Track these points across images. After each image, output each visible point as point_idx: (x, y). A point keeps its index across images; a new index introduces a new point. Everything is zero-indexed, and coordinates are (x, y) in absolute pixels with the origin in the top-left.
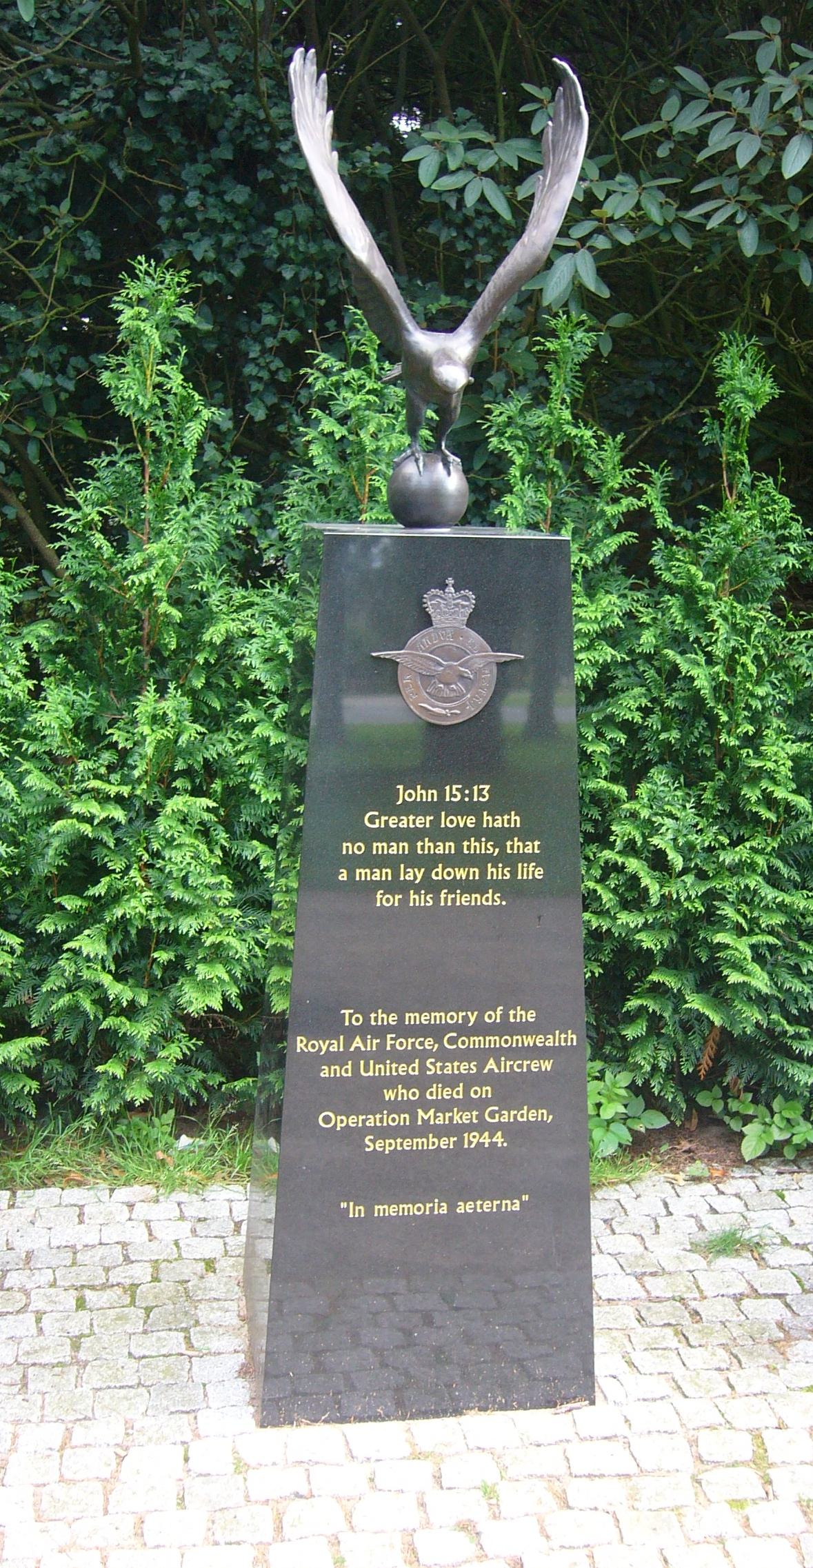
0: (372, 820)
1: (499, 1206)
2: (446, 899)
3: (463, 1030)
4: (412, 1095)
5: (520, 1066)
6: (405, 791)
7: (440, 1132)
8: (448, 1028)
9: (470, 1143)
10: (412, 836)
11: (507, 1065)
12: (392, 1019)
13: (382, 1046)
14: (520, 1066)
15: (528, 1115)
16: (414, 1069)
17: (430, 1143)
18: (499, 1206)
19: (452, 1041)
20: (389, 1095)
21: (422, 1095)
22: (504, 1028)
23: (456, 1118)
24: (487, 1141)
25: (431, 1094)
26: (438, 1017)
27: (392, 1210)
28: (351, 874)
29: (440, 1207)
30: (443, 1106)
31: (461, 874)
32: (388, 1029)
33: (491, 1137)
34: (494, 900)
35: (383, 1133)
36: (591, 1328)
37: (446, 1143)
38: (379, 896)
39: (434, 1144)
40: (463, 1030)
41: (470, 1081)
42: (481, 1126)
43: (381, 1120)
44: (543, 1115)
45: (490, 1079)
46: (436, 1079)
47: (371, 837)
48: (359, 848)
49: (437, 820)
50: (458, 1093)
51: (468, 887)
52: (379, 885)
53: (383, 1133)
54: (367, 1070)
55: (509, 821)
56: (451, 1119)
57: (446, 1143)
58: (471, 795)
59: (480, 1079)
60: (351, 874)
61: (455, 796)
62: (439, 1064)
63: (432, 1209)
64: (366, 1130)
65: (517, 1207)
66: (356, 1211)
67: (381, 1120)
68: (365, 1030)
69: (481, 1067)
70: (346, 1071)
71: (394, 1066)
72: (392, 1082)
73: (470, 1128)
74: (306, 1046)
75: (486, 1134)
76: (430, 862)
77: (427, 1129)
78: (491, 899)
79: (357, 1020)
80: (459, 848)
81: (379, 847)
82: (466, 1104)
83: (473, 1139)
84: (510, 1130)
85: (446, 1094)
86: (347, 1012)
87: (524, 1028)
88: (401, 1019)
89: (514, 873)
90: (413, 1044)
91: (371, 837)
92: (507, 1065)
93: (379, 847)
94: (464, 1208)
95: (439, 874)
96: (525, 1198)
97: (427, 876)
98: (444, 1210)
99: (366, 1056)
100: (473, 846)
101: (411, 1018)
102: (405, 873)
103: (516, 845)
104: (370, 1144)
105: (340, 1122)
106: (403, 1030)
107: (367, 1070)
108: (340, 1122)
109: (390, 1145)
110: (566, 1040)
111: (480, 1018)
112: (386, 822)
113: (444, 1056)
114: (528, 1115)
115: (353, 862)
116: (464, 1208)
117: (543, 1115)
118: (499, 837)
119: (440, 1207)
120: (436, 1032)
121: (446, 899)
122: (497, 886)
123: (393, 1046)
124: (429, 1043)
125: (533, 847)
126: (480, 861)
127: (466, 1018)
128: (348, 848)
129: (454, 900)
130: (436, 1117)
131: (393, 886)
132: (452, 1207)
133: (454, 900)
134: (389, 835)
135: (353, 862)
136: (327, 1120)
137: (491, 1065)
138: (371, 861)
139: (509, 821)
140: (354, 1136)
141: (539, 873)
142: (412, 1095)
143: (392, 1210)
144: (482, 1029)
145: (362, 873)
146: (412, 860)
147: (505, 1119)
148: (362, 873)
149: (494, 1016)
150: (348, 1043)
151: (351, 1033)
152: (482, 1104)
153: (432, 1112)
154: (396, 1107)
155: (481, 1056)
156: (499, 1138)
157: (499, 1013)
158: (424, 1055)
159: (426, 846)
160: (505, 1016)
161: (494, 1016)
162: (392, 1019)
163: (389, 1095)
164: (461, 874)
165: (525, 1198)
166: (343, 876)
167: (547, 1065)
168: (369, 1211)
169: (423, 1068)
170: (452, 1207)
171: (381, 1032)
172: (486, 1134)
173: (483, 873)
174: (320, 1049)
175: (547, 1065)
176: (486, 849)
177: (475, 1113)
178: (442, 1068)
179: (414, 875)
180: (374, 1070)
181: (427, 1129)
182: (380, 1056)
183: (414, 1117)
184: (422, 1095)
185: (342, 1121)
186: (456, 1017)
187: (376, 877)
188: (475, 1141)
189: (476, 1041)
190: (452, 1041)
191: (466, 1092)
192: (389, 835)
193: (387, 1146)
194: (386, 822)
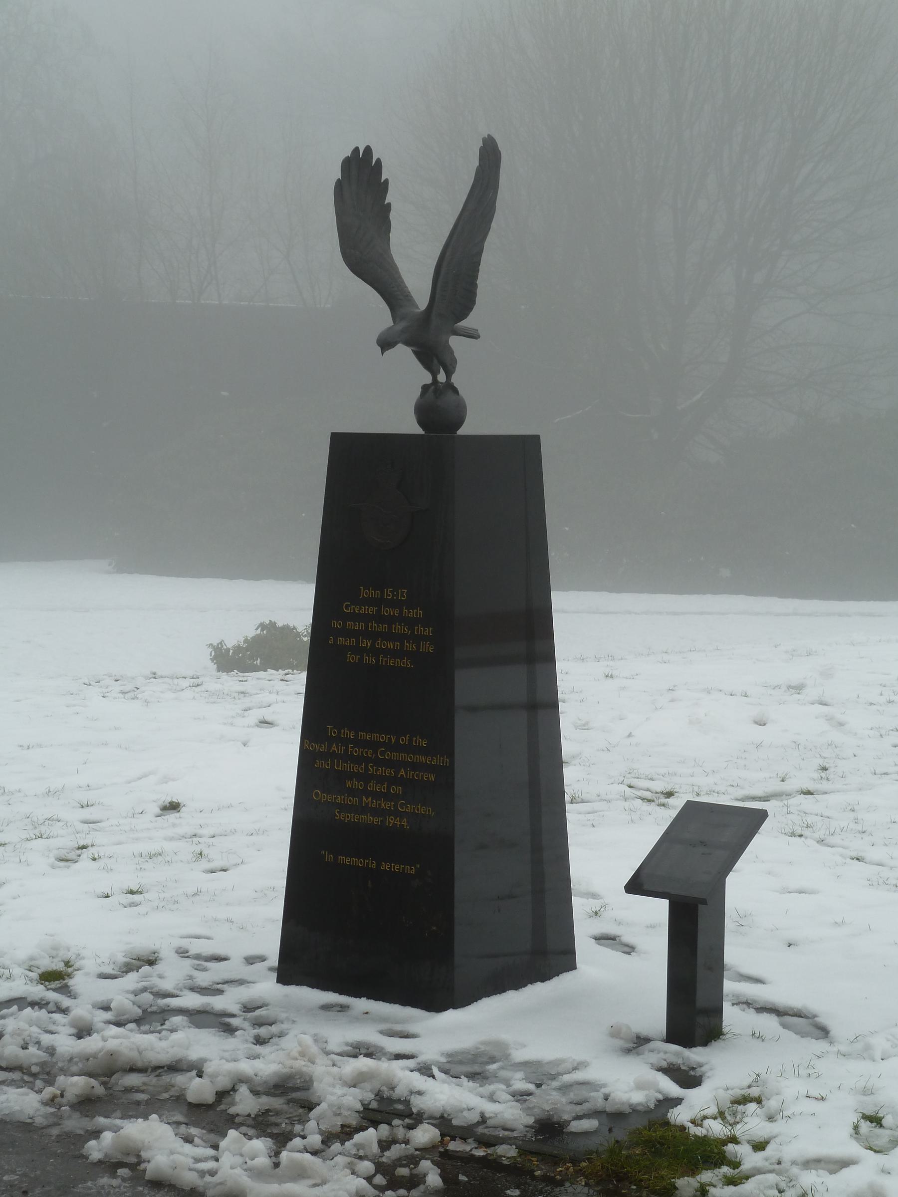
0: (347, 608)
1: (404, 869)
4: (360, 786)
7: (376, 812)
9: (389, 823)
17: (368, 819)
20: (349, 784)
26: (376, 736)
28: (335, 640)
30: (376, 795)
31: (390, 645)
54: (338, 766)
56: (380, 804)
60: (335, 640)
63: (368, 863)
66: (329, 858)
78: (405, 663)
83: (391, 821)
89: (418, 647)
94: (385, 866)
98: (374, 866)
100: (399, 628)
107: (338, 766)
112: (354, 609)
116: (385, 866)
125: (428, 631)
127: (390, 739)
129: (386, 661)
133: (386, 661)
134: (355, 617)
137: (402, 772)
142: (360, 786)
148: (341, 640)
149: (404, 740)
154: (352, 792)
160: (410, 740)
161: (404, 740)
163: (349, 784)
164: (390, 645)
167: (432, 778)
168: (336, 859)
186: (384, 738)
189: (395, 756)
190: (383, 753)
192: (355, 617)
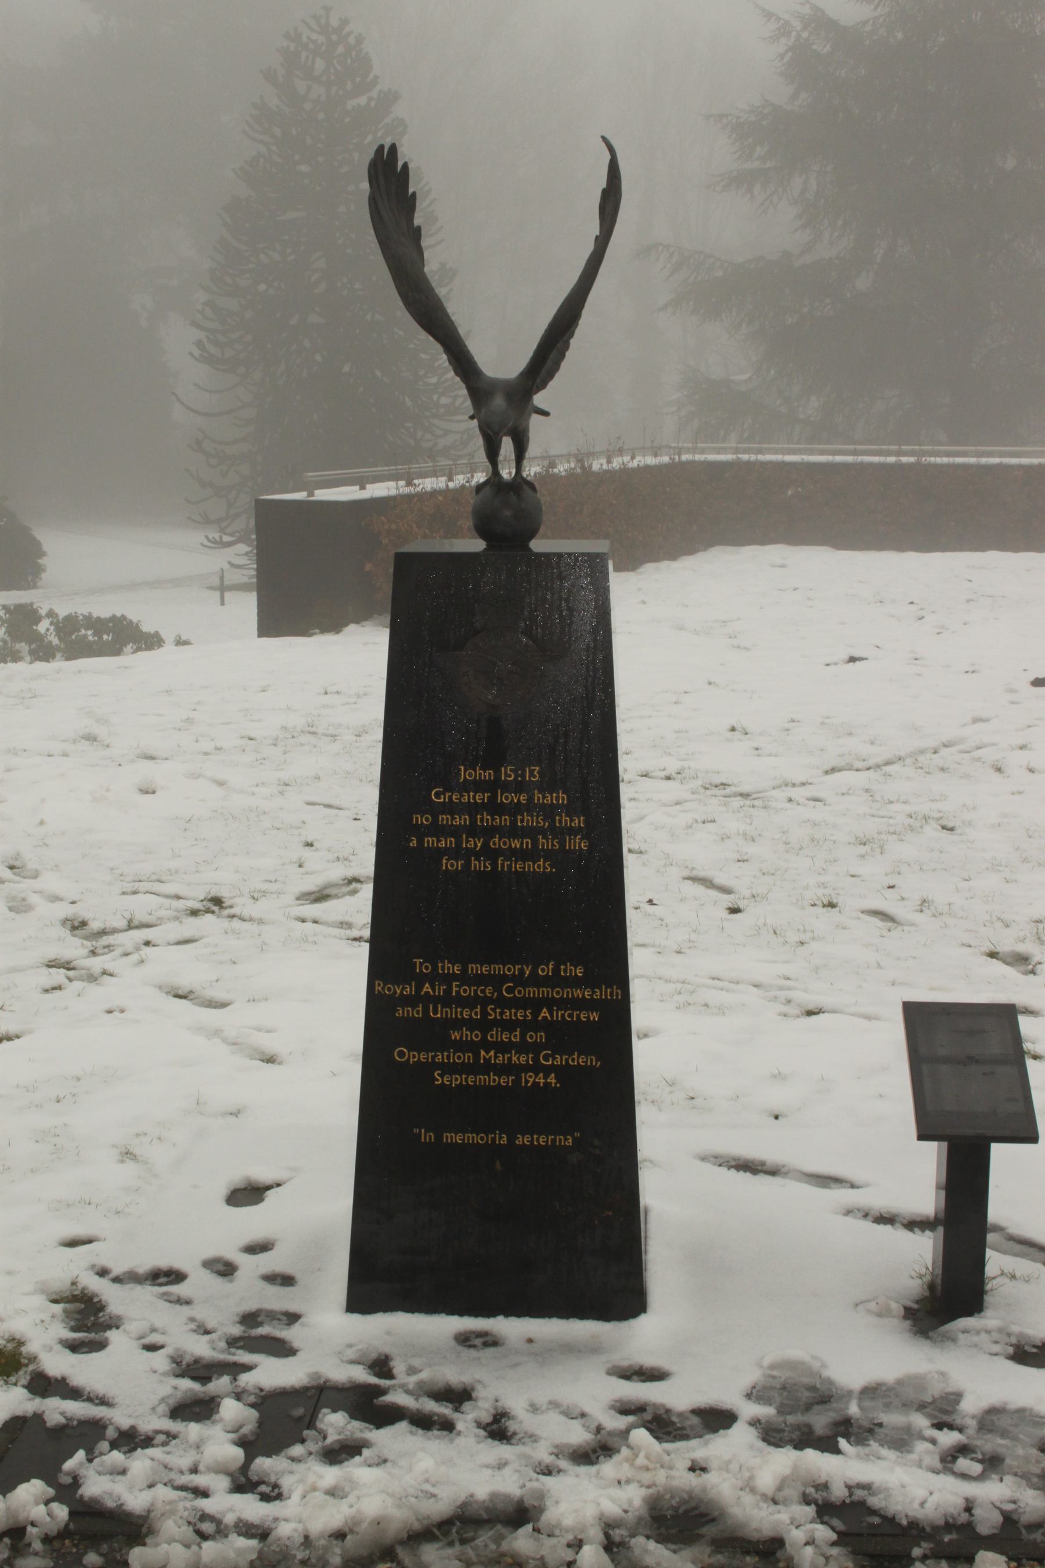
0: (437, 795)
1: (554, 1141)
2: (503, 865)
3: (519, 980)
4: (476, 1036)
5: (570, 1016)
6: (465, 771)
8: (504, 979)
9: (527, 1082)
10: (473, 809)
11: (558, 1015)
12: (457, 969)
13: (448, 991)
14: (570, 1016)
15: (578, 1060)
16: (476, 1014)
17: (492, 1080)
18: (554, 1141)
19: (510, 990)
20: (455, 1035)
21: (484, 1037)
22: (555, 980)
23: (514, 1059)
24: (542, 1081)
25: (492, 1036)
26: (497, 969)
27: (458, 1138)
28: (420, 842)
29: (500, 1138)
30: (502, 1048)
31: (516, 844)
32: (454, 977)
33: (545, 1078)
34: (545, 868)
35: (449, 1069)
36: (375, 941)
38: (444, 861)
39: (494, 1080)
40: (519, 980)
41: (526, 1026)
43: (448, 1057)
44: (593, 1061)
45: (547, 1025)
46: (495, 1023)
47: (435, 810)
48: (427, 819)
49: (494, 796)
50: (516, 1037)
51: (523, 855)
52: (446, 851)
53: (449, 1069)
54: (435, 1013)
55: (557, 799)
56: (510, 1059)
58: (523, 776)
59: (534, 1025)
60: (420, 842)
61: (510, 776)
62: (498, 1010)
63: (494, 1139)
64: (434, 1065)
66: (427, 1136)
67: (448, 1057)
68: (433, 978)
69: (536, 1013)
70: (417, 1013)
71: (459, 1010)
72: (458, 1024)
73: (526, 1068)
74: (383, 989)
75: (541, 1075)
76: (490, 832)
77: (488, 1067)
78: (541, 866)
79: (427, 968)
80: (473, 821)
81: (444, 819)
82: (523, 1047)
83: (530, 1079)
84: (561, 1072)
86: (418, 961)
87: (575, 982)
88: (464, 970)
89: (562, 844)
90: (475, 991)
91: (435, 810)
92: (558, 1015)
93: (444, 819)
95: (496, 842)
96: (577, 1134)
97: (485, 845)
98: (504, 1140)
99: (436, 1000)
100: (526, 820)
101: (474, 968)
102: (467, 841)
103: (526, 818)
105: (414, 1057)
106: (464, 979)
107: (435, 1013)
108: (414, 1057)
109: (456, 1079)
110: (611, 994)
111: (534, 972)
112: (450, 798)
113: (502, 1003)
114: (578, 1060)
115: (421, 832)
117: (593, 1061)
118: (550, 812)
119: (500, 1138)
120: (498, 981)
121: (503, 865)
122: (548, 855)
123: (458, 992)
125: (578, 822)
126: (532, 833)
127: (522, 971)
129: (510, 867)
130: (496, 1057)
131: (456, 853)
132: (511, 1140)
133: (510, 867)
134: (450, 808)
135: (421, 832)
136: (401, 1054)
137: (545, 1013)
138: (438, 831)
139: (557, 799)
140: (426, 1069)
142: (476, 1036)
143: (458, 1138)
144: (536, 981)
145: (430, 841)
146: (472, 831)
147: (558, 1062)
148: (430, 841)
149: (545, 970)
150: (419, 988)
152: (536, 1048)
153: (492, 1053)
155: (536, 1005)
156: (552, 1079)
157: (551, 967)
158: (485, 1002)
159: (485, 819)
160: (556, 970)
161: (545, 970)
162: (457, 969)
163: (455, 1035)
164: (516, 844)
165: (577, 1134)
166: (414, 843)
167: (595, 1016)
168: (439, 1137)
169: (484, 1013)
172: (541, 1075)
173: (535, 842)
174: (395, 992)
175: (595, 1016)
176: (538, 822)
177: (530, 1056)
178: (501, 1014)
180: (440, 1013)
181: (488, 1067)
182: (447, 1000)
183: (477, 1055)
184: (484, 1037)
185: (414, 1056)
187: (442, 844)
188: (531, 1080)
189: (531, 992)
190: (510, 990)
191: (523, 1036)
192: (450, 808)
193: (456, 1080)
194: (450, 798)
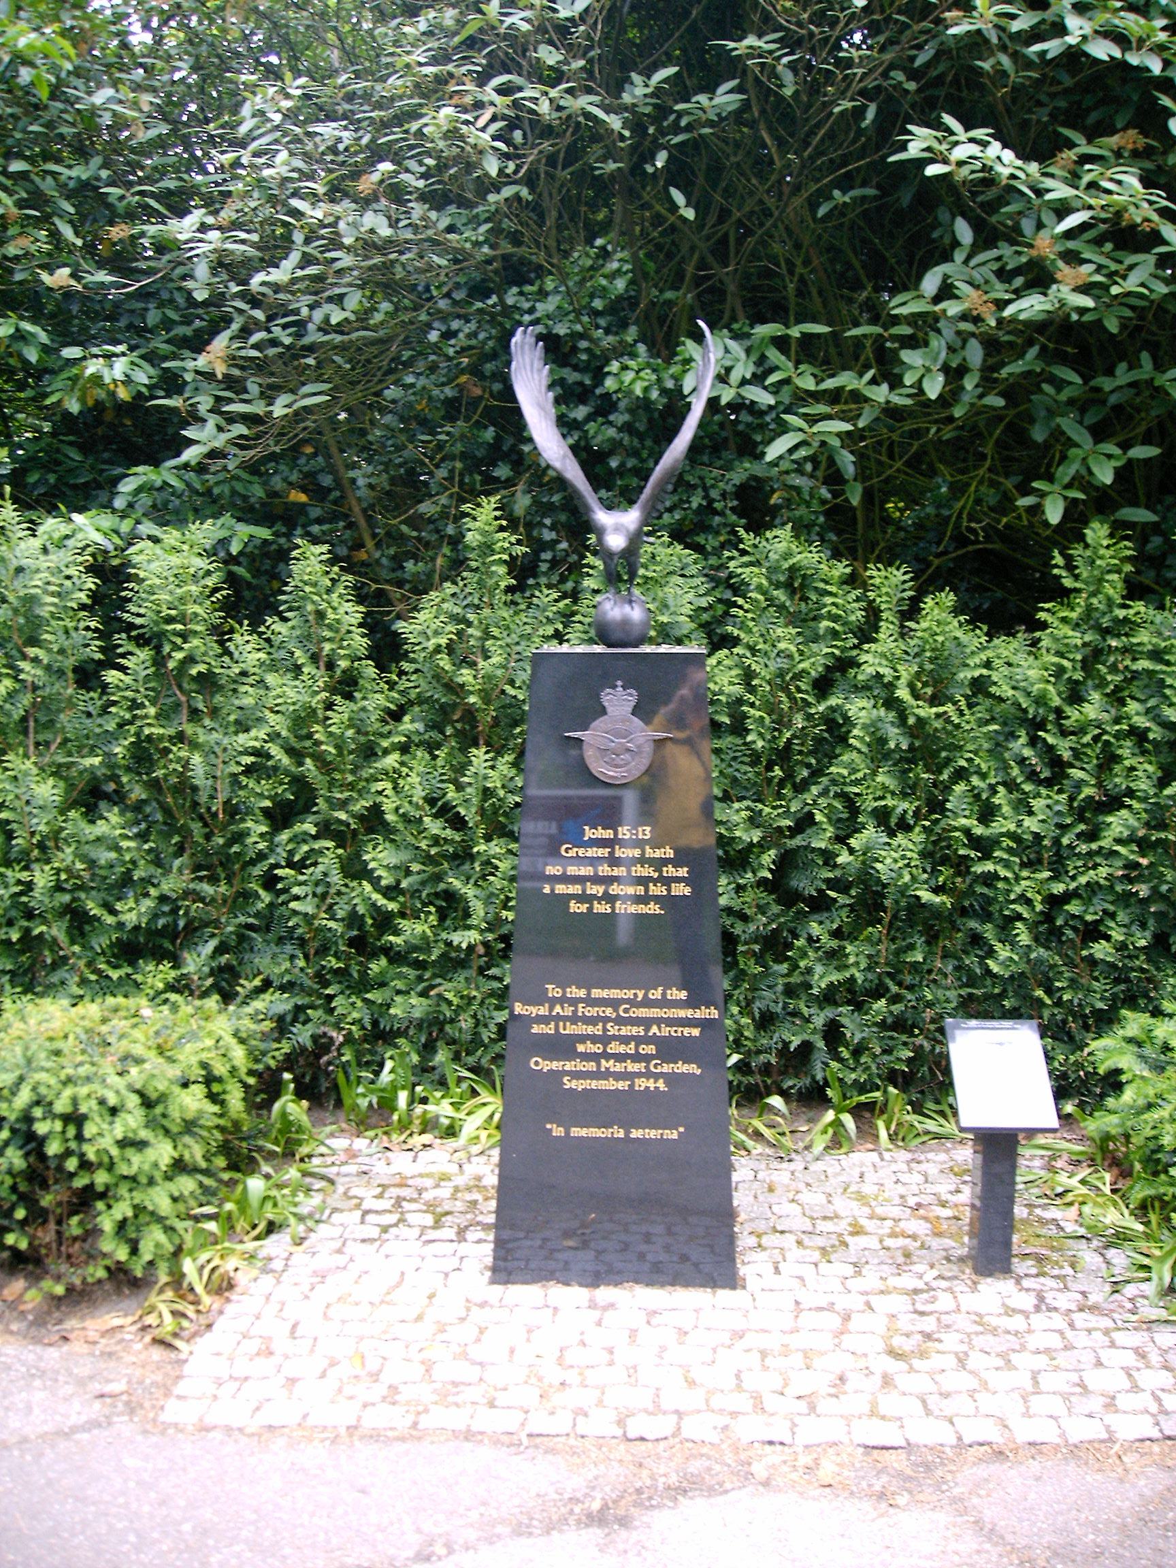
3: (633, 1003)
4: (597, 1048)
7: (618, 1076)
10: (593, 861)
11: (666, 1031)
12: (582, 993)
16: (598, 1030)
20: (581, 1048)
22: (664, 1003)
26: (615, 993)
27: (583, 1132)
30: (620, 1058)
32: (581, 1000)
37: (622, 1085)
40: (633, 1003)
41: (639, 1040)
42: (648, 1075)
46: (614, 1038)
57: (622, 1085)
59: (647, 1040)
65: (675, 1136)
66: (558, 1131)
68: (563, 1000)
69: (647, 1030)
70: (550, 1029)
72: (583, 1039)
73: (639, 1075)
77: (607, 1075)
81: (572, 870)
82: (637, 1057)
83: (642, 1084)
84: (670, 1078)
85: (622, 1049)
94: (635, 1134)
99: (565, 1019)
101: (597, 993)
104: (569, 1083)
105: (546, 1066)
106: (591, 1002)
108: (546, 1066)
113: (620, 1021)
114: (682, 1068)
116: (635, 1134)
117: (693, 1069)
120: (614, 1003)
122: (657, 899)
124: (609, 1011)
125: (683, 872)
128: (551, 870)
132: (627, 1133)
137: (654, 1029)
138: (565, 879)
140: (557, 1075)
141: (687, 891)
142: (597, 1048)
143: (583, 1132)
144: (647, 1003)
145: (560, 889)
146: (597, 880)
148: (560, 889)
149: (656, 994)
151: (553, 1002)
152: (647, 1058)
154: (586, 1057)
155: (647, 1023)
156: (661, 1084)
158: (606, 1020)
161: (656, 994)
162: (582, 993)
163: (581, 1048)
167: (696, 1032)
170: (627, 1133)
171: (574, 1002)
175: (696, 1032)
179: (598, 890)
180: (571, 1029)
181: (607, 1075)
182: (574, 1019)
186: (629, 994)
189: (643, 1012)
